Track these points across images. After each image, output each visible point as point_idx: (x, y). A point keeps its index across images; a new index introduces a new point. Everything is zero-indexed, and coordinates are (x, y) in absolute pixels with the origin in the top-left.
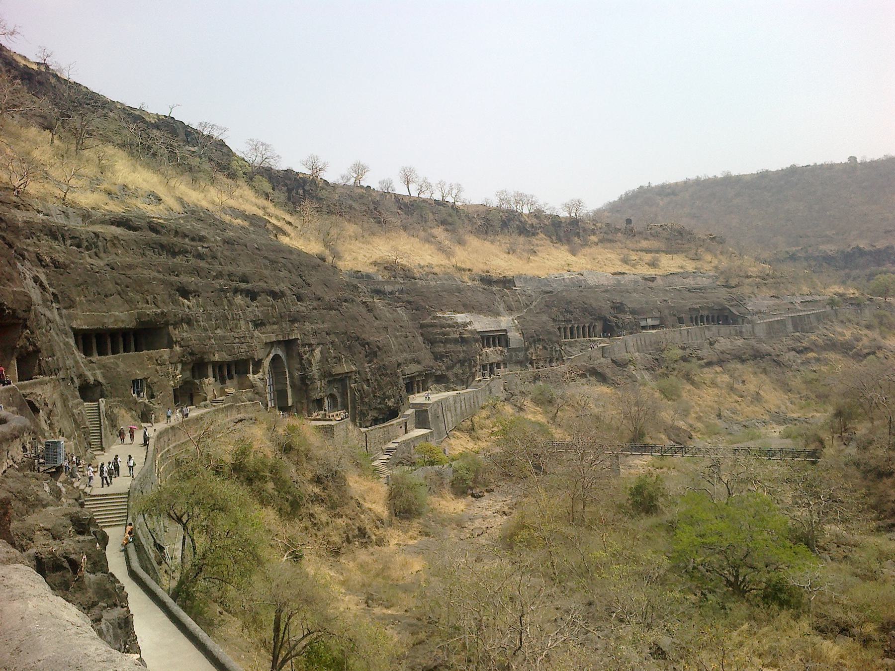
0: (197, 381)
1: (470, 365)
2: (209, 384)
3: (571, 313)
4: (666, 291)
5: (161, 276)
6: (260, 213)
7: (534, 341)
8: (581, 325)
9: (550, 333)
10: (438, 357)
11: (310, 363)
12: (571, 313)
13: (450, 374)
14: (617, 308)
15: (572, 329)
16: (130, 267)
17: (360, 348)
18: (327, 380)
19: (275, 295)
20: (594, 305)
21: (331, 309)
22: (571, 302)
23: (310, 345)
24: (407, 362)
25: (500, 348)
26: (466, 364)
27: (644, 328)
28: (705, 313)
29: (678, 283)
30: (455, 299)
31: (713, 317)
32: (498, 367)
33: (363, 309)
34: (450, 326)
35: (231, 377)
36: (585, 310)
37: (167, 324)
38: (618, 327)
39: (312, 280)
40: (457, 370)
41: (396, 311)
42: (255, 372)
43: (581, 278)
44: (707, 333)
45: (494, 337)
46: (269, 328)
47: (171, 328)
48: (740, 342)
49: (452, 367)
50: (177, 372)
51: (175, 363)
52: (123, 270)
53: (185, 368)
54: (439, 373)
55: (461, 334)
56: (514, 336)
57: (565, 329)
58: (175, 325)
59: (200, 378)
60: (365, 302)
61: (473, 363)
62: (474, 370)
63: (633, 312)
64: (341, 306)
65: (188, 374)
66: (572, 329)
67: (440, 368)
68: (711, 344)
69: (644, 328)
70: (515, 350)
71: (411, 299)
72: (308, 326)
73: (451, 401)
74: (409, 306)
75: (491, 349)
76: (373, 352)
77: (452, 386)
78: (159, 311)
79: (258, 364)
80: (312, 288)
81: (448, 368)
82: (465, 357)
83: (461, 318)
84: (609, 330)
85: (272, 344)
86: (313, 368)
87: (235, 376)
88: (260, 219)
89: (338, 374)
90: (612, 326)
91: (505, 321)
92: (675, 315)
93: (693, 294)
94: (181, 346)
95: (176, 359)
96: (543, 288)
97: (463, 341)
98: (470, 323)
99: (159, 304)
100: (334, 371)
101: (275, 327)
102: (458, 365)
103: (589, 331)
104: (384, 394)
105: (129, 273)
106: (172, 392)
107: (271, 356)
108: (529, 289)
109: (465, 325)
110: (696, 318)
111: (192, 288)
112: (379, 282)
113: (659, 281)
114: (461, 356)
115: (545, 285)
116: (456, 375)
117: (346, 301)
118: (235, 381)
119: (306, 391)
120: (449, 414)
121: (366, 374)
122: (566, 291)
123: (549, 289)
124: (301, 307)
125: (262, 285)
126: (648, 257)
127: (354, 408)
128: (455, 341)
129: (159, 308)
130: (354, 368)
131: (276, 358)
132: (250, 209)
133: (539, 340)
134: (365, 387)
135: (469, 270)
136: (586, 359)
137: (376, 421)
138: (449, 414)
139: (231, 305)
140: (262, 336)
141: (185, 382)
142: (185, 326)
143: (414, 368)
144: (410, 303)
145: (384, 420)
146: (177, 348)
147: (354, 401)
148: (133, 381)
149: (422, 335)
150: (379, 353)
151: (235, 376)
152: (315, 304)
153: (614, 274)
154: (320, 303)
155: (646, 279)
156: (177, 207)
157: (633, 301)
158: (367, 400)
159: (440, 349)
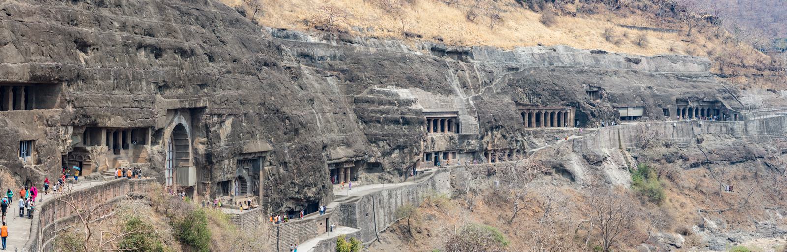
0: (89, 148)
1: (411, 151)
2: (100, 154)
3: (538, 95)
4: (652, 76)
5: (59, 25)
7: (492, 129)
8: (550, 112)
9: (511, 119)
10: (373, 140)
11: (219, 137)
12: (538, 95)
13: (385, 162)
14: (594, 92)
15: (538, 115)
16: (29, 14)
17: (279, 123)
18: (236, 159)
19: (183, 53)
20: (567, 88)
21: (248, 73)
22: (539, 82)
23: (220, 116)
24: (334, 144)
25: (449, 134)
27: (623, 119)
28: (693, 105)
29: (667, 67)
30: (398, 71)
31: (703, 110)
32: (446, 155)
33: (286, 76)
34: (390, 103)
35: (126, 147)
36: (554, 93)
37: (61, 81)
38: (594, 116)
39: (229, 38)
40: (396, 155)
41: (325, 80)
42: (154, 143)
43: (554, 54)
44: (695, 128)
45: (443, 121)
46: (172, 92)
47: (65, 84)
48: (730, 141)
49: (390, 154)
50: (68, 136)
51: (66, 126)
52: (21, 16)
53: (77, 132)
54: (372, 160)
55: (403, 113)
56: (470, 123)
57: (530, 115)
58: (70, 82)
59: (92, 145)
60: (289, 68)
61: (415, 150)
62: (415, 158)
63: (612, 99)
64: (260, 70)
65: (79, 139)
66: (538, 115)
67: (376, 154)
68: (699, 142)
69: (623, 119)
70: (466, 137)
71: (345, 67)
72: (220, 93)
73: (385, 194)
74: (342, 76)
75: (439, 134)
76: (296, 129)
77: (387, 176)
78: (54, 64)
79: (158, 133)
80: (228, 48)
81: (384, 154)
82: (405, 143)
83: (404, 93)
84: (582, 119)
85: (175, 111)
86: (222, 144)
87: (131, 145)
89: (251, 154)
90: (587, 116)
91: (459, 102)
92: (660, 106)
93: (683, 83)
94: (74, 107)
95: (68, 121)
96: (506, 63)
97: (407, 122)
98: (414, 101)
99: (54, 57)
100: (246, 149)
101: (181, 91)
103: (559, 119)
104: (304, 181)
105: (26, 20)
106: (60, 159)
107: (174, 125)
108: (490, 64)
109: (408, 102)
110: (684, 110)
111: (90, 40)
112: (308, 45)
113: (644, 65)
114: (401, 141)
115: (510, 60)
116: (393, 163)
117: (266, 65)
118: (131, 152)
119: (211, 172)
120: (381, 212)
121: (284, 155)
122: (535, 69)
123: (514, 65)
124: (212, 68)
125: (170, 40)
126: (634, 34)
127: (266, 195)
128: (396, 122)
129: (54, 61)
130: (269, 147)
131: (179, 128)
133: (497, 127)
134: (282, 171)
135: (419, 36)
136: (553, 153)
137: (291, 213)
139: (134, 62)
140: (165, 101)
141: (76, 149)
142: (80, 83)
143: (341, 153)
144: (343, 71)
146: (70, 109)
147: (266, 188)
148: (21, 142)
149: (355, 111)
150: (301, 131)
151: (131, 145)
152: (230, 66)
153: (592, 52)
154: (235, 65)
155: (629, 61)
157: (612, 85)
158: (282, 187)
159: (376, 130)
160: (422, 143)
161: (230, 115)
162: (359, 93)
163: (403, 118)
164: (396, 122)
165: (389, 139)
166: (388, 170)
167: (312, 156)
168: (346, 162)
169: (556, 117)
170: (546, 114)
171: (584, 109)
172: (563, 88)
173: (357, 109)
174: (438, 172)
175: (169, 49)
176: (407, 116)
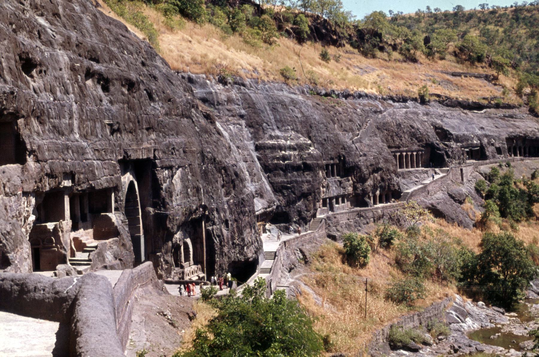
38: (448, 156)
87: (88, 215)
90: (442, 156)
111: (38, 58)
151: (88, 215)
160: (322, 189)
161: (179, 167)
163: (305, 164)
165: (293, 186)
166: (295, 220)
167: (248, 211)
171: (439, 149)
172: (418, 129)
173: (260, 156)
175: (116, 79)
176: (308, 162)
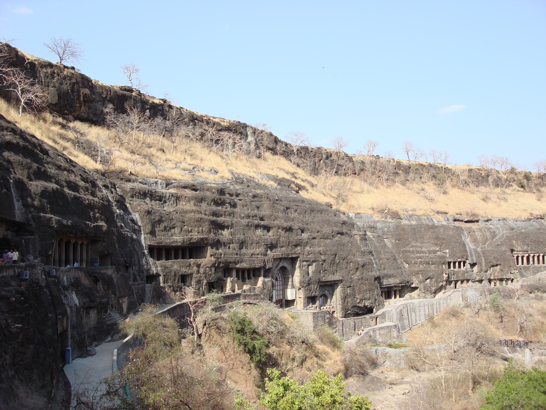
6: (288, 177)
7: (493, 266)
13: (421, 286)
15: (528, 258)
26: (434, 280)
35: (249, 278)
41: (384, 241)
54: (413, 286)
57: (522, 257)
65: (220, 274)
66: (528, 258)
81: (420, 282)
82: (434, 275)
88: (288, 181)
102: (428, 281)
120: (413, 314)
125: (277, 222)
132: (282, 175)
133: (497, 265)
138: (413, 314)
145: (363, 314)
156: (228, 175)
160: (444, 275)
162: (404, 247)
164: (428, 263)
168: (394, 286)
169: (541, 258)
170: (533, 257)
174: (453, 292)
